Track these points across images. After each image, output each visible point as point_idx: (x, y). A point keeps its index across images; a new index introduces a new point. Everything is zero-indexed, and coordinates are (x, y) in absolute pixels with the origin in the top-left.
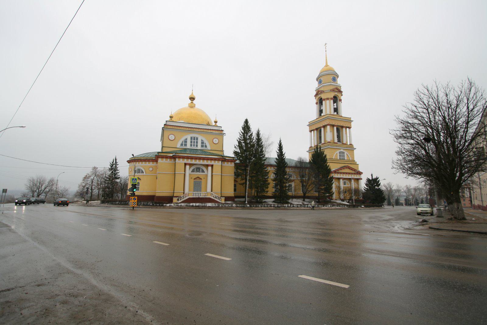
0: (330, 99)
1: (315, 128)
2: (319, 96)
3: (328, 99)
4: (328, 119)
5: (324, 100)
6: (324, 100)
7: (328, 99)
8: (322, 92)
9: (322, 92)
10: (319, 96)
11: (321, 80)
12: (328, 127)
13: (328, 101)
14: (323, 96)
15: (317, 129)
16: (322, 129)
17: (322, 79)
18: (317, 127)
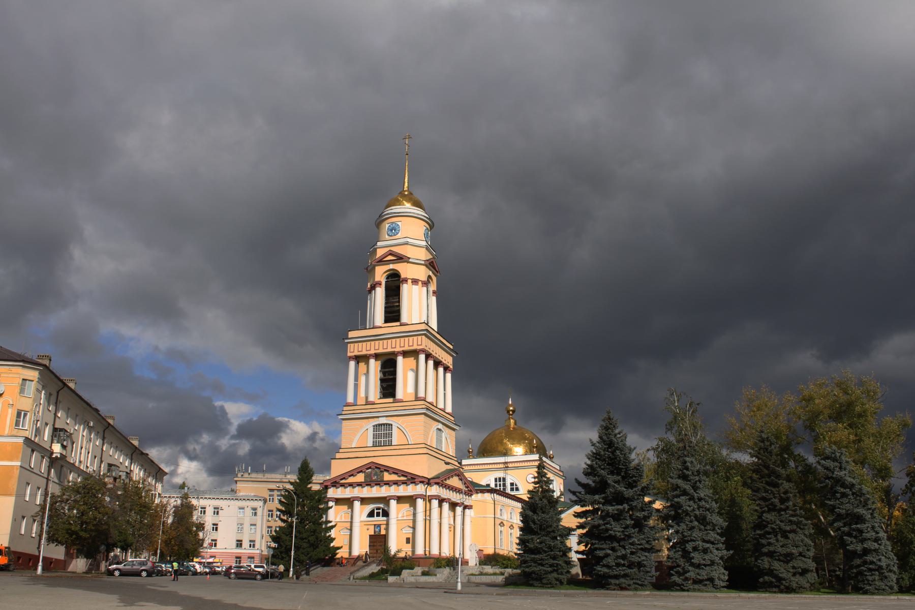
0: (420, 283)
1: (373, 352)
2: (391, 266)
3: (415, 282)
4: (423, 337)
5: (406, 280)
6: (406, 280)
7: (415, 282)
8: (402, 258)
9: (400, 258)
10: (391, 266)
11: (398, 225)
12: (422, 357)
13: (416, 288)
14: (404, 270)
15: (377, 356)
16: (400, 359)
17: (399, 223)
18: (381, 351)
